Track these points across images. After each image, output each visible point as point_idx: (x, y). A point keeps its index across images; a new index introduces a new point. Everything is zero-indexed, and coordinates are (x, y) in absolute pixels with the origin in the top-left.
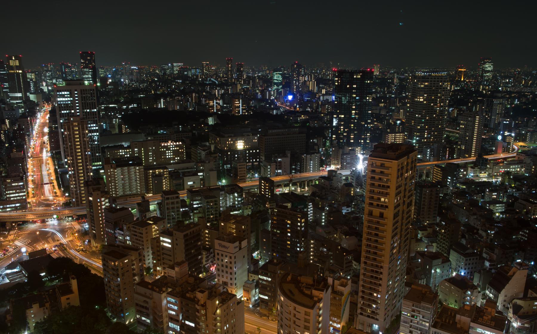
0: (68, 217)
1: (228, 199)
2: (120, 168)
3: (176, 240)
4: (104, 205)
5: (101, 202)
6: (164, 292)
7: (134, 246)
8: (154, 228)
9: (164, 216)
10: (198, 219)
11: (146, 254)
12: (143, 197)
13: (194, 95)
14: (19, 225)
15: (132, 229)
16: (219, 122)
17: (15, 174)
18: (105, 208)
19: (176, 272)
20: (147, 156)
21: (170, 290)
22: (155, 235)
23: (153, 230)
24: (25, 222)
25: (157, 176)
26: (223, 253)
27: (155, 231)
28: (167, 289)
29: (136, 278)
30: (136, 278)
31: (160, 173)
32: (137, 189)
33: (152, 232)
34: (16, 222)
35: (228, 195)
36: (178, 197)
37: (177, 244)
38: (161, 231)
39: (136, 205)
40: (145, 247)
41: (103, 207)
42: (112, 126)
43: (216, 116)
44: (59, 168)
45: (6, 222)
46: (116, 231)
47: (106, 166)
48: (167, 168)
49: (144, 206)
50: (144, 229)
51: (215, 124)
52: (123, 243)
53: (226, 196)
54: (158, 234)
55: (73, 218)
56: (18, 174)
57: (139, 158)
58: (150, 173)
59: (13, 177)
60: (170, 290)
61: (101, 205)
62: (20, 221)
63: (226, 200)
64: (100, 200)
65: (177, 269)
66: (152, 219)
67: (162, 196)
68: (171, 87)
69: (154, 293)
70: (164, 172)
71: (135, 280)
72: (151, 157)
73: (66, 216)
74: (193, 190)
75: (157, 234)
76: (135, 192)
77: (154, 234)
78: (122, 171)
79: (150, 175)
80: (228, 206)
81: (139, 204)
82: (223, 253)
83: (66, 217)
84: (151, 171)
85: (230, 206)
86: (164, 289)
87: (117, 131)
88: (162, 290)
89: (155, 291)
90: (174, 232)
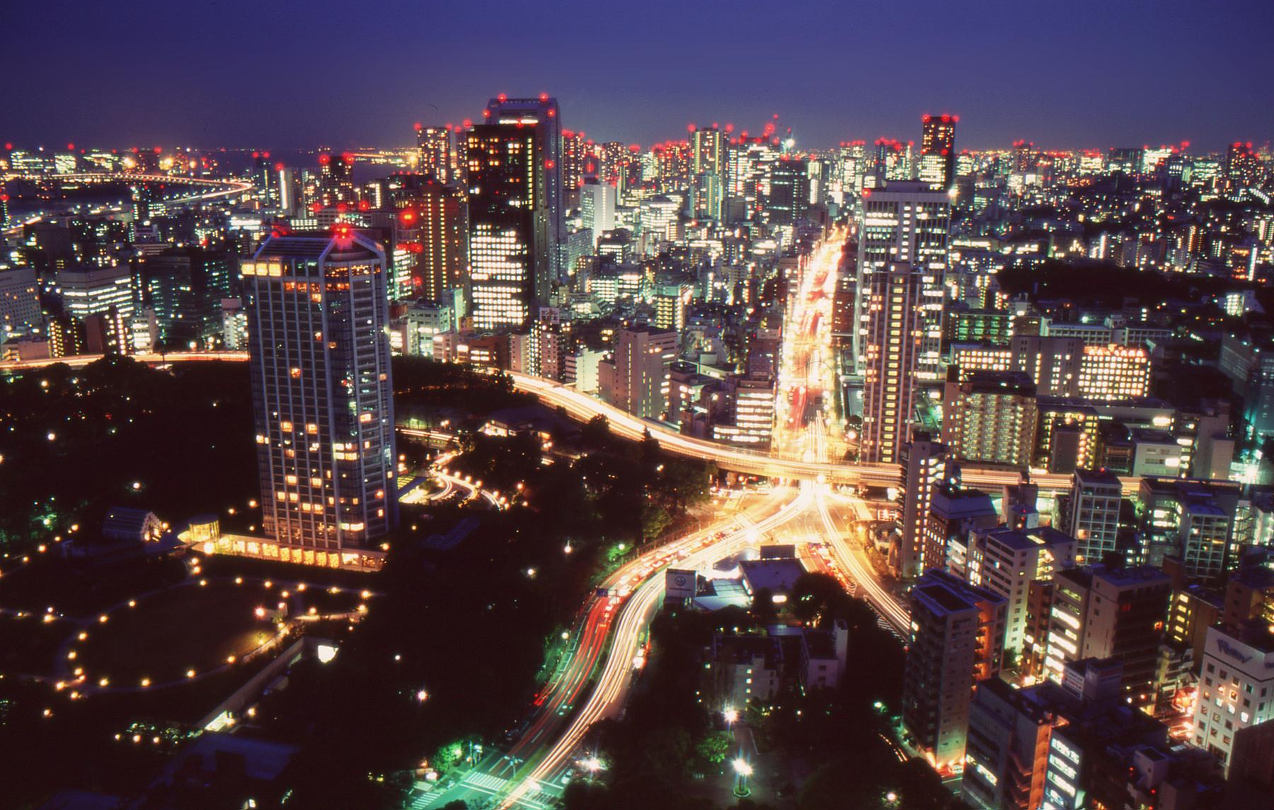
0: (848, 486)
1: (1259, 523)
2: (979, 395)
3: (1098, 600)
4: (934, 475)
5: (927, 466)
6: (1046, 722)
7: (986, 587)
8: (1043, 556)
9: (1069, 530)
10: (1165, 562)
11: (1011, 614)
12: (1025, 475)
13: (1193, 230)
14: (750, 482)
15: (988, 545)
16: (1260, 310)
17: (760, 373)
18: (934, 484)
19: (1087, 682)
20: (1047, 374)
21: (1062, 722)
22: (1043, 574)
23: (1040, 561)
24: (761, 479)
25: (1065, 427)
26: (1214, 662)
27: (1045, 564)
28: (1054, 720)
29: (981, 666)
30: (981, 666)
31: (1075, 422)
32: (1010, 451)
33: (1035, 564)
34: (746, 475)
35: (1261, 513)
36: (1116, 492)
37: (1097, 613)
38: (1061, 569)
39: (1005, 491)
40: (1013, 597)
41: (931, 480)
42: (973, 294)
43: (1253, 293)
44: (844, 374)
45: (728, 471)
46: (949, 543)
47: (948, 386)
48: (1094, 413)
49: (1023, 497)
50: (1018, 553)
51: (1245, 314)
52: (962, 574)
53: (1254, 515)
54: (1050, 573)
55: (857, 491)
56: (765, 374)
57: (1027, 377)
58: (1049, 417)
59: (756, 380)
60: (1062, 722)
61: (926, 475)
62: (752, 475)
63: (1252, 527)
64: (927, 463)
65: (1091, 675)
66: (1041, 533)
67: (1074, 480)
68: (1130, 207)
69: (1020, 715)
70: (1085, 421)
71: (978, 671)
72: (1055, 378)
73: (845, 482)
74: (1159, 480)
75: (1047, 574)
76: (1004, 457)
77: (1039, 570)
78: (983, 403)
79: (1048, 424)
80: (1255, 543)
81: (1011, 489)
82: (1214, 662)
83: (842, 485)
84: (1053, 414)
85: (1261, 545)
86: (1049, 716)
87: (982, 304)
88: (1042, 717)
89: (1025, 713)
90: (1096, 579)
